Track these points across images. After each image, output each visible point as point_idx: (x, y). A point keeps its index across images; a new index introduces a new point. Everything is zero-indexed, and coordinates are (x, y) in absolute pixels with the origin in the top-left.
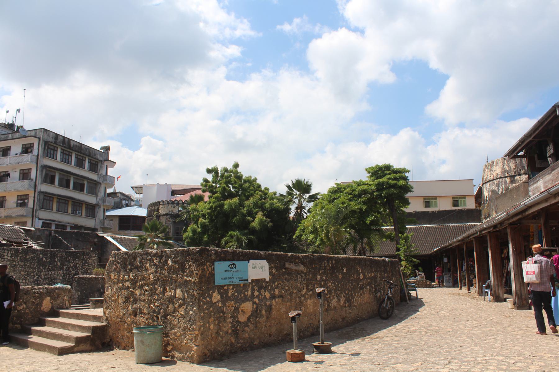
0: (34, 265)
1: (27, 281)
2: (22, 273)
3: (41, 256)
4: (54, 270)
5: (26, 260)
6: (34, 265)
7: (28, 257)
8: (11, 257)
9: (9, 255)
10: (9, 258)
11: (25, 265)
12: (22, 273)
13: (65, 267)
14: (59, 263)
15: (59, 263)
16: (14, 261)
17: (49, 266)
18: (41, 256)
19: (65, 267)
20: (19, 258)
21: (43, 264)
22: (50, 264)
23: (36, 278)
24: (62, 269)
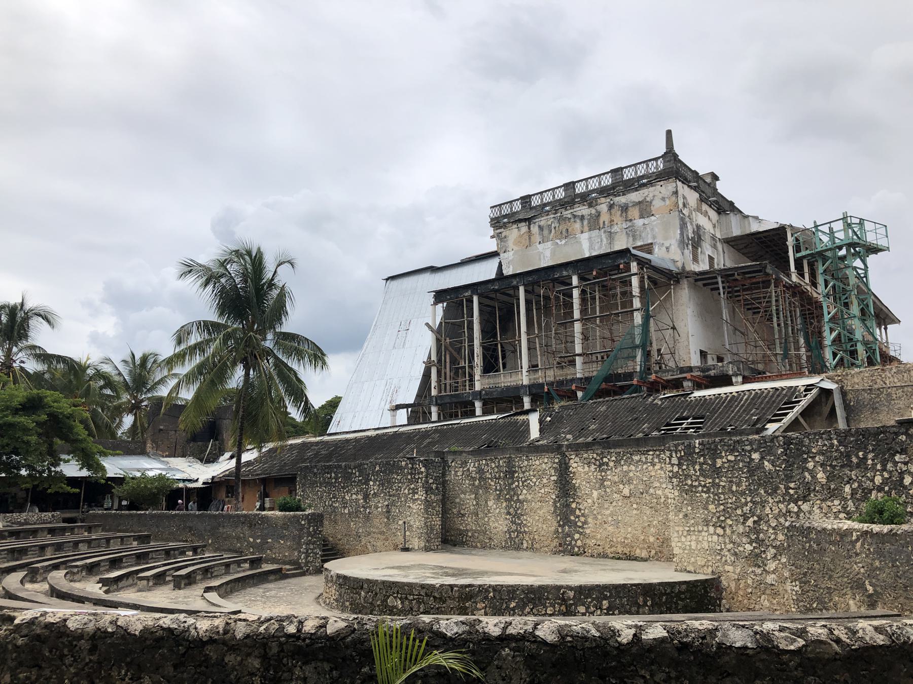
0: (738, 485)
1: (728, 531)
2: (711, 507)
3: (756, 456)
4: (805, 499)
5: (717, 471)
6: (738, 485)
7: (719, 463)
8: (680, 465)
9: (675, 461)
10: (676, 469)
11: (714, 484)
12: (711, 507)
13: (847, 489)
14: (821, 476)
15: (821, 476)
16: (687, 476)
17: (787, 488)
18: (756, 456)
19: (847, 489)
20: (697, 467)
21: (768, 483)
22: (789, 478)
23: (750, 522)
24: (833, 494)
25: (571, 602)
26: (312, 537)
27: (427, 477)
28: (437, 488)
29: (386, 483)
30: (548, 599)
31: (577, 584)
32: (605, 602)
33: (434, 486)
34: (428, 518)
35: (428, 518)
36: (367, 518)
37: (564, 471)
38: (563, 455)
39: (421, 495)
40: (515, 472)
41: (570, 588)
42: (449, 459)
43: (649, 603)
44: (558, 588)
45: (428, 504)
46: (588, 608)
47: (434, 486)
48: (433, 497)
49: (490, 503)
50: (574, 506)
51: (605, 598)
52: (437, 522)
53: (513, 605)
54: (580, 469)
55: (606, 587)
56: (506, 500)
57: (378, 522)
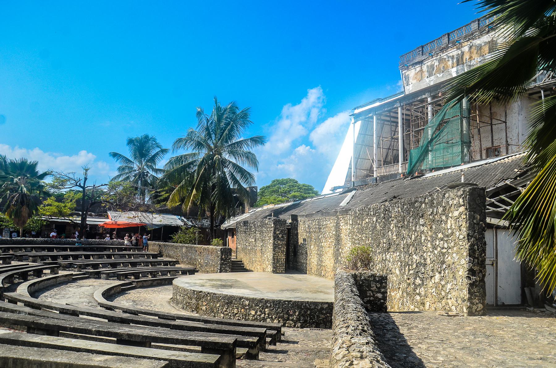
25: (247, 307)
26: (224, 261)
27: (275, 230)
28: (282, 237)
29: (261, 232)
30: (235, 304)
31: (252, 297)
32: (266, 310)
33: (280, 236)
34: (275, 254)
35: (275, 254)
36: (255, 253)
37: (337, 227)
38: (338, 219)
39: (271, 241)
40: (321, 228)
41: (247, 299)
42: (299, 219)
43: (297, 314)
44: (241, 298)
45: (275, 247)
46: (256, 313)
47: (280, 236)
48: (279, 242)
49: (312, 247)
50: (340, 251)
51: (267, 307)
52: (283, 257)
53: (218, 305)
54: (344, 227)
55: (267, 301)
56: (318, 246)
57: (259, 255)
